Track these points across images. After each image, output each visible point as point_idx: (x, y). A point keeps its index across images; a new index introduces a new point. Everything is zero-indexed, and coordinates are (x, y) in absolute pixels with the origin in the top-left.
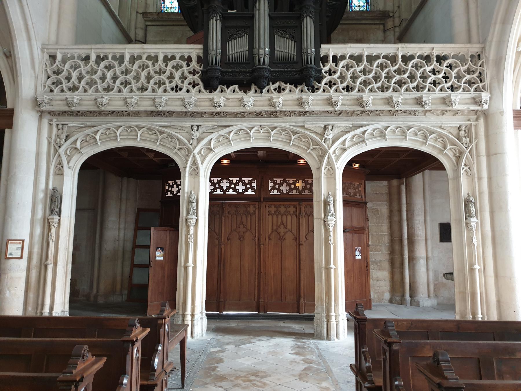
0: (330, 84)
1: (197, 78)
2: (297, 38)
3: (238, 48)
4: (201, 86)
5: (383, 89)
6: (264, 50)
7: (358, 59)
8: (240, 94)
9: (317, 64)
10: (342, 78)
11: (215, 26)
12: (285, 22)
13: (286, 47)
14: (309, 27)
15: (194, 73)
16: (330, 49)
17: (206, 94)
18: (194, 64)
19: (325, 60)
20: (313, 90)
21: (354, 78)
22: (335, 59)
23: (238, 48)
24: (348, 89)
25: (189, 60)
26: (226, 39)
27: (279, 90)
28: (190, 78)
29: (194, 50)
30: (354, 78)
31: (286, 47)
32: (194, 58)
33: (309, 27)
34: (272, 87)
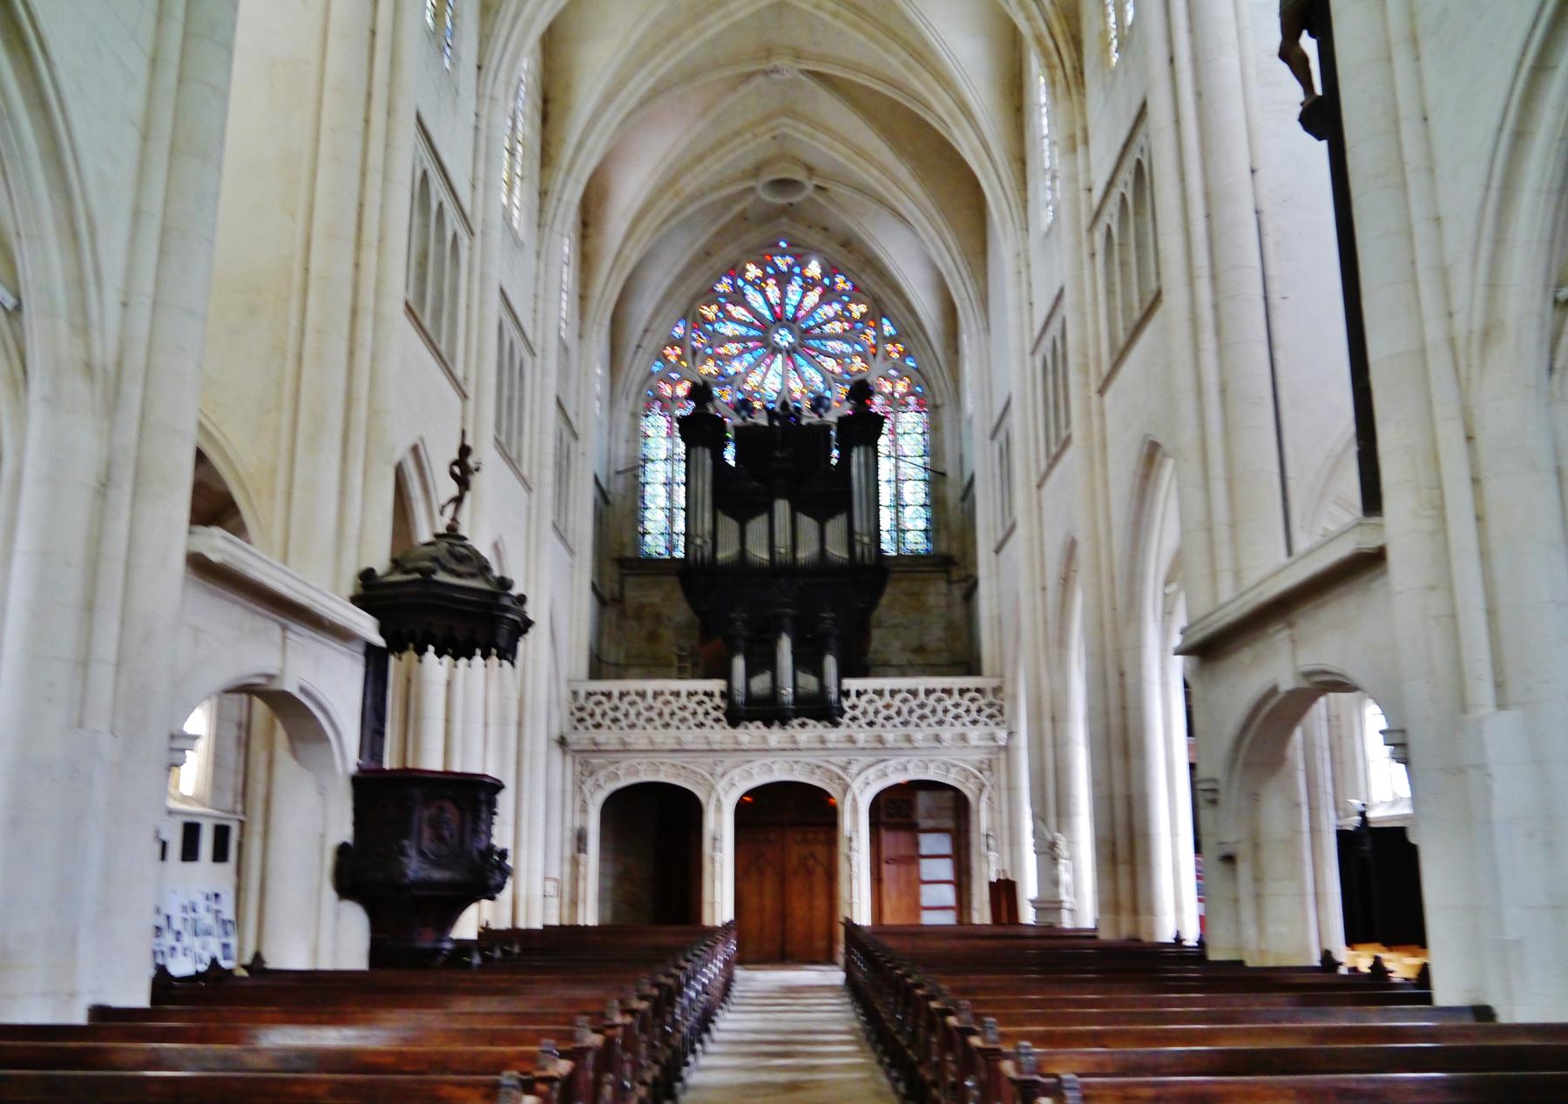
0: (854, 719)
1: (720, 714)
2: (819, 673)
3: (761, 683)
4: (725, 723)
5: (905, 723)
6: (787, 692)
7: (880, 693)
8: (764, 730)
9: (839, 701)
10: (865, 713)
11: (739, 664)
12: (807, 660)
13: (809, 682)
14: (830, 664)
15: (717, 708)
16: (851, 684)
17: (730, 730)
18: (718, 700)
19: (847, 694)
20: (836, 725)
21: (876, 712)
22: (859, 694)
23: (761, 683)
24: (871, 724)
25: (710, 695)
26: (750, 673)
27: (803, 725)
28: (715, 714)
29: (717, 685)
30: (876, 712)
31: (809, 682)
32: (717, 694)
33: (830, 664)
34: (795, 722)
